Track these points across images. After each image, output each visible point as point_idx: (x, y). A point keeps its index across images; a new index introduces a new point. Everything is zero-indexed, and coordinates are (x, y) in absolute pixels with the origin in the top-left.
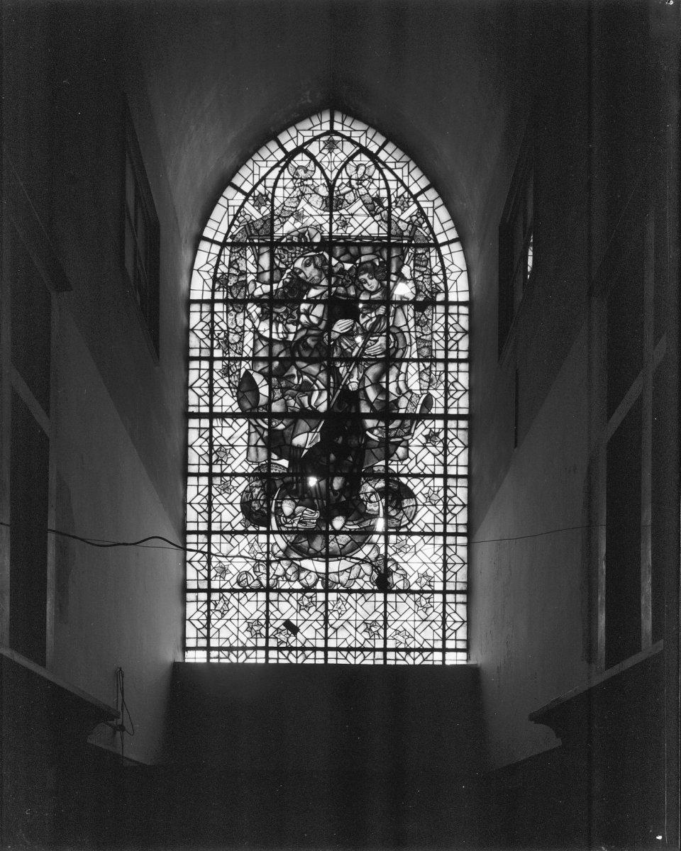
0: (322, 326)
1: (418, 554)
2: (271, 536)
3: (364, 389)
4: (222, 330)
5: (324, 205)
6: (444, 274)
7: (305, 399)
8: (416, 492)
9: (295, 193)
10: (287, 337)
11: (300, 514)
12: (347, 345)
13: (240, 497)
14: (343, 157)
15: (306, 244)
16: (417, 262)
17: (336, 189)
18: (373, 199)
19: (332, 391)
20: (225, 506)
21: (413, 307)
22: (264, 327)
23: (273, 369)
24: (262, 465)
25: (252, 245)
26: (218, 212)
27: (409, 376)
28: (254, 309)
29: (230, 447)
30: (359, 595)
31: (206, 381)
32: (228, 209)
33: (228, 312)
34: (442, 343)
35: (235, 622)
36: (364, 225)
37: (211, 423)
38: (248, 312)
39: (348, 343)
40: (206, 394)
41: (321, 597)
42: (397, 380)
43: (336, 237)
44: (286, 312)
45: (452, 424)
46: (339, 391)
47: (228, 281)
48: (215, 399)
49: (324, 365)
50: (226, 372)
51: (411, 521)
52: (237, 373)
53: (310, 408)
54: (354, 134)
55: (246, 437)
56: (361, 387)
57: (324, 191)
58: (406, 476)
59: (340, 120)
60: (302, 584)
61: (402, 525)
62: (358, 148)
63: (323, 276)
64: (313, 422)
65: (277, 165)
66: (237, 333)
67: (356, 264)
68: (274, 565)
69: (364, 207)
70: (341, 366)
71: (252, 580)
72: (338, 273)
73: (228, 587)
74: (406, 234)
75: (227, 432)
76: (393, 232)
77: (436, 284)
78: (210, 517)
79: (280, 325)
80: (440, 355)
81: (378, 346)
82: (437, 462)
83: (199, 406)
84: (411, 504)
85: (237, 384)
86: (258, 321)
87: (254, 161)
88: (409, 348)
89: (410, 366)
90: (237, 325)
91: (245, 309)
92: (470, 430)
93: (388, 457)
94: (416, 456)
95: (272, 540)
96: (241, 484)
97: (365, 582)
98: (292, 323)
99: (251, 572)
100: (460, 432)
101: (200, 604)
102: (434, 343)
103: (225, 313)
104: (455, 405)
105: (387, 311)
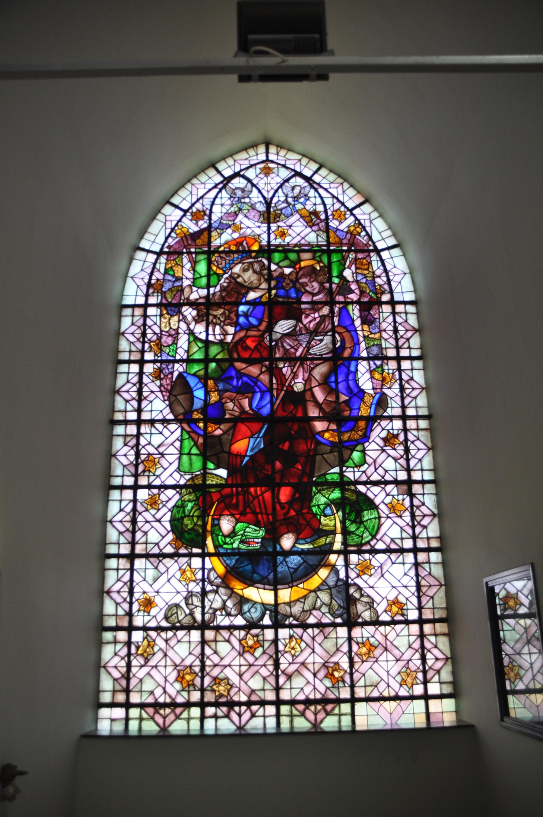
0: (263, 327)
1: (385, 576)
2: (207, 559)
3: (311, 389)
4: (155, 333)
5: (262, 219)
6: (388, 276)
7: (245, 403)
8: (377, 501)
9: (232, 209)
10: (225, 339)
11: (242, 532)
12: (290, 345)
13: (170, 513)
14: (279, 180)
15: (244, 251)
16: (358, 266)
17: (273, 205)
18: (311, 213)
19: (275, 393)
20: (152, 523)
21: (358, 307)
22: (199, 329)
23: (209, 371)
24: (196, 475)
25: (189, 253)
26: (156, 226)
27: (359, 375)
28: (189, 312)
29: (160, 456)
30: (316, 631)
31: (135, 385)
32: (165, 223)
33: (161, 315)
34: (393, 341)
35: (162, 669)
36: (302, 235)
37: (139, 429)
38: (183, 315)
39: (291, 344)
40: (134, 399)
41: (269, 634)
42: (347, 380)
43: (274, 245)
44: (224, 313)
45: (411, 424)
46: (283, 392)
47: (162, 286)
48: (144, 403)
49: (266, 366)
50: (157, 375)
51: (374, 537)
52: (170, 376)
53: (250, 412)
54: (288, 162)
55: (177, 444)
56: (308, 387)
57: (262, 208)
58: (364, 483)
59: (275, 152)
60: (245, 619)
61: (363, 542)
62: (293, 173)
63: (262, 280)
64: (255, 426)
65: (215, 186)
66: (170, 335)
67: (296, 269)
68: (211, 596)
69: (301, 220)
70: (284, 367)
71: (183, 615)
72: (278, 277)
73: (153, 624)
74: (344, 241)
75: (157, 440)
76: (331, 240)
77: (380, 286)
78: (134, 537)
79: (218, 328)
80: (392, 353)
81: (323, 345)
82: (399, 467)
83: (126, 411)
84: (373, 516)
85: (169, 388)
86: (194, 323)
87: (193, 184)
88: (357, 346)
89: (359, 365)
90: (171, 328)
91: (180, 312)
92: (430, 430)
93: (342, 463)
94: (375, 461)
95: (208, 565)
96: (171, 497)
97: (323, 614)
98: (230, 325)
99: (183, 604)
100: (421, 433)
101: (119, 646)
102: (383, 341)
103: (158, 317)
104: (413, 404)
105: (332, 311)
